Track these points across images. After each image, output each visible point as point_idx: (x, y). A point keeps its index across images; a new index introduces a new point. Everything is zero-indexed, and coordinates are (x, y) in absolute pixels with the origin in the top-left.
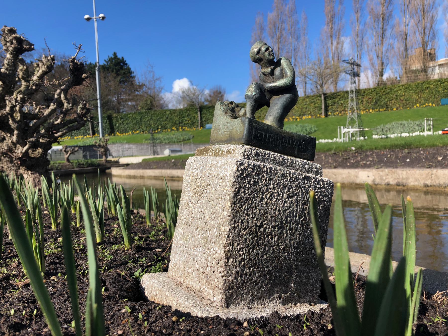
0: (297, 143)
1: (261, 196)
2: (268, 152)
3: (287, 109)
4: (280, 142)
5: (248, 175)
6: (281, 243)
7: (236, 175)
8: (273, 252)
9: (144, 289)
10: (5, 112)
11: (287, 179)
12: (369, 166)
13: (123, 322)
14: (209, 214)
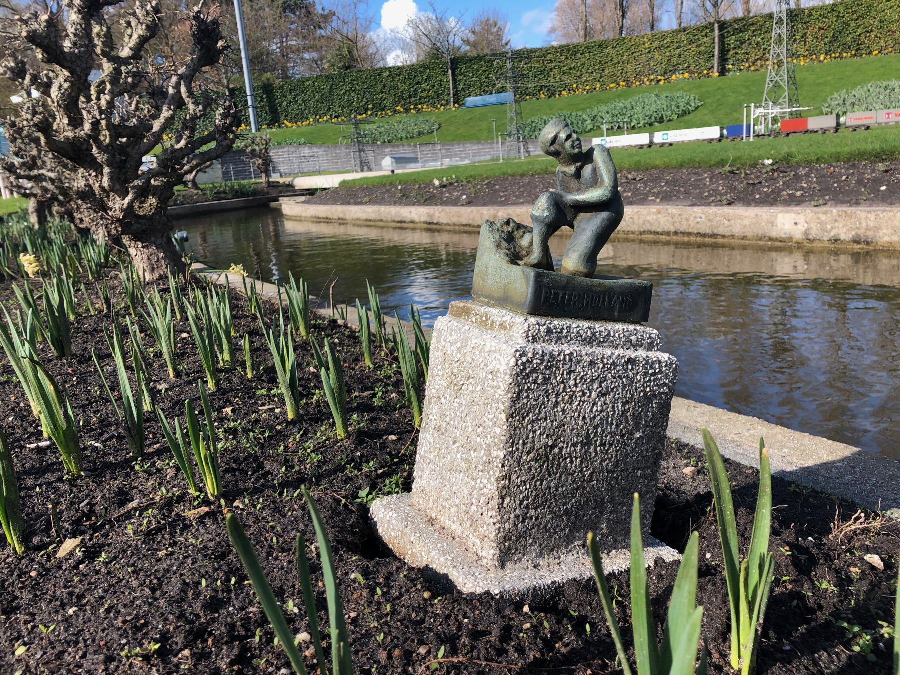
0: (618, 298)
1: (554, 400)
3: (602, 238)
5: (534, 371)
6: (587, 467)
8: (573, 482)
9: (375, 524)
10: (82, 133)
12: (799, 202)
13: (355, 596)
14: (472, 425)
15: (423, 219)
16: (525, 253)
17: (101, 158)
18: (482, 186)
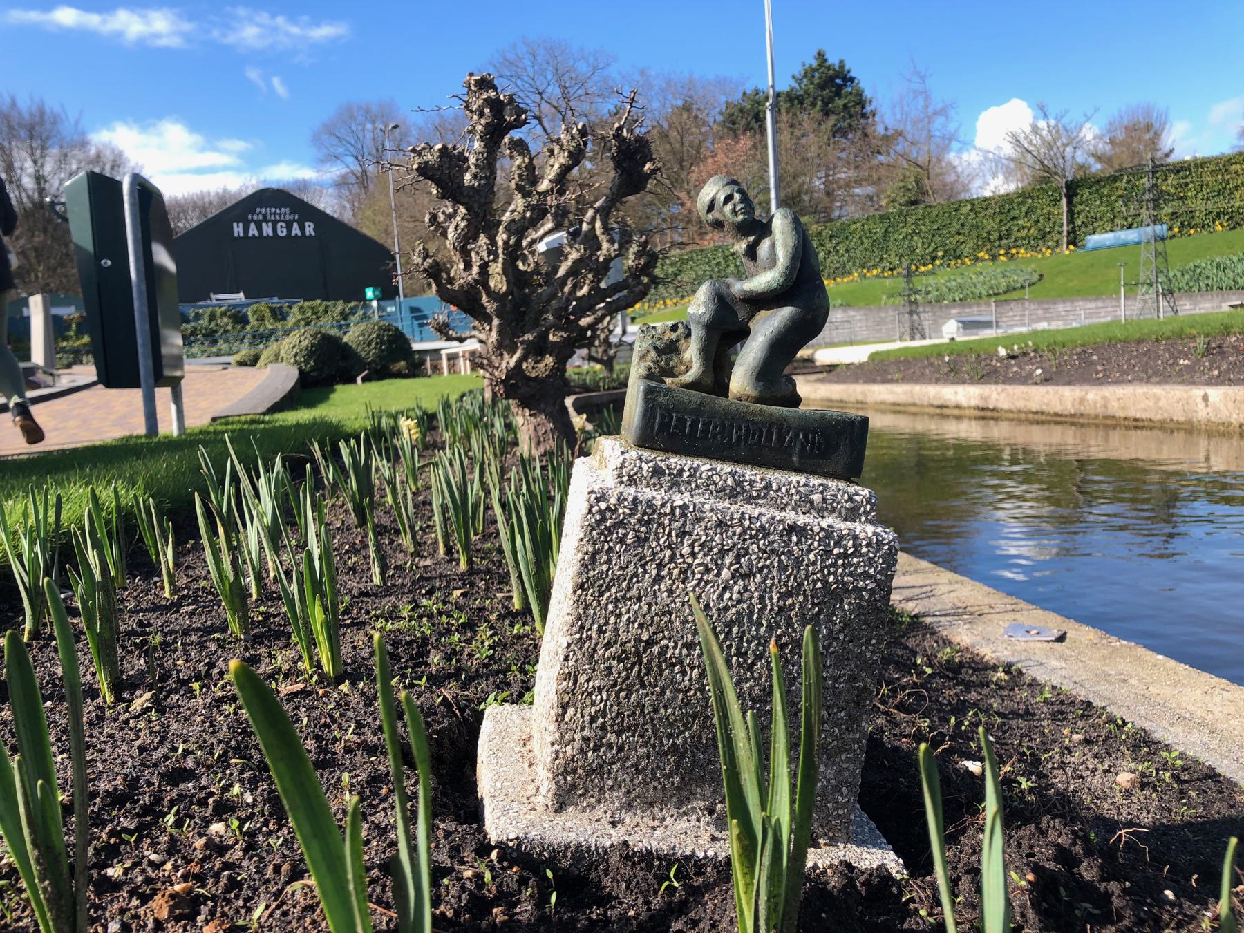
0: (796, 435)
1: (654, 572)
4: (739, 437)
5: (619, 524)
11: (734, 534)
15: (973, 403)
16: (683, 368)
17: (490, 306)
18: (1071, 356)
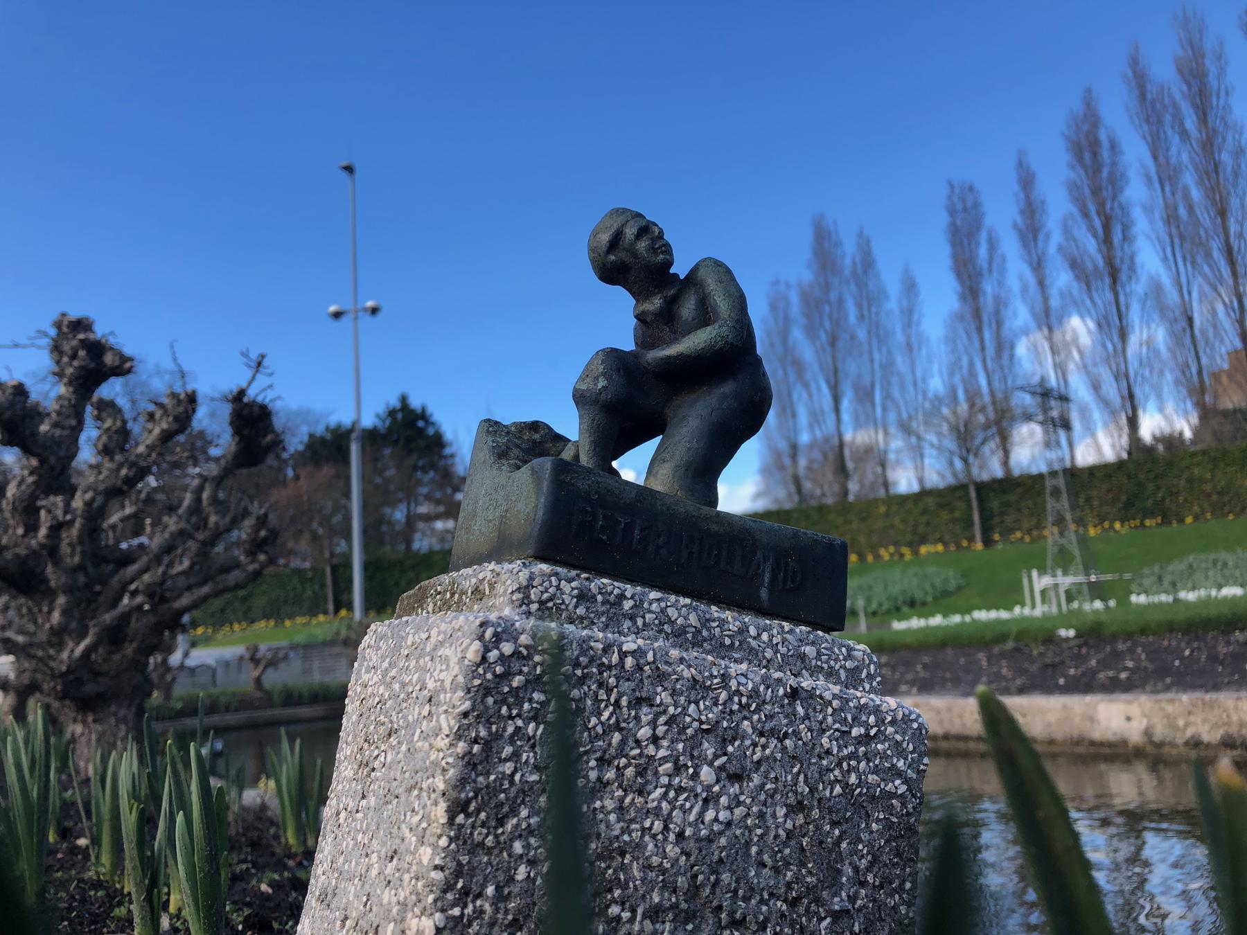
2: (629, 590)
7: (477, 682)
